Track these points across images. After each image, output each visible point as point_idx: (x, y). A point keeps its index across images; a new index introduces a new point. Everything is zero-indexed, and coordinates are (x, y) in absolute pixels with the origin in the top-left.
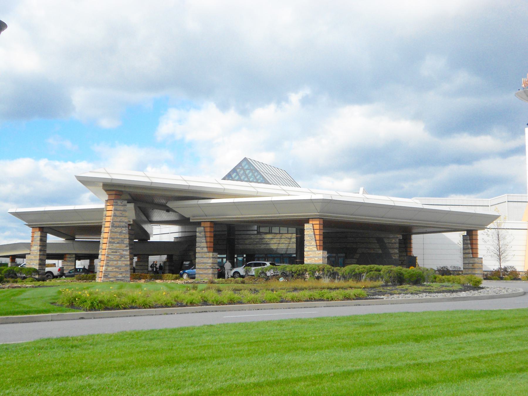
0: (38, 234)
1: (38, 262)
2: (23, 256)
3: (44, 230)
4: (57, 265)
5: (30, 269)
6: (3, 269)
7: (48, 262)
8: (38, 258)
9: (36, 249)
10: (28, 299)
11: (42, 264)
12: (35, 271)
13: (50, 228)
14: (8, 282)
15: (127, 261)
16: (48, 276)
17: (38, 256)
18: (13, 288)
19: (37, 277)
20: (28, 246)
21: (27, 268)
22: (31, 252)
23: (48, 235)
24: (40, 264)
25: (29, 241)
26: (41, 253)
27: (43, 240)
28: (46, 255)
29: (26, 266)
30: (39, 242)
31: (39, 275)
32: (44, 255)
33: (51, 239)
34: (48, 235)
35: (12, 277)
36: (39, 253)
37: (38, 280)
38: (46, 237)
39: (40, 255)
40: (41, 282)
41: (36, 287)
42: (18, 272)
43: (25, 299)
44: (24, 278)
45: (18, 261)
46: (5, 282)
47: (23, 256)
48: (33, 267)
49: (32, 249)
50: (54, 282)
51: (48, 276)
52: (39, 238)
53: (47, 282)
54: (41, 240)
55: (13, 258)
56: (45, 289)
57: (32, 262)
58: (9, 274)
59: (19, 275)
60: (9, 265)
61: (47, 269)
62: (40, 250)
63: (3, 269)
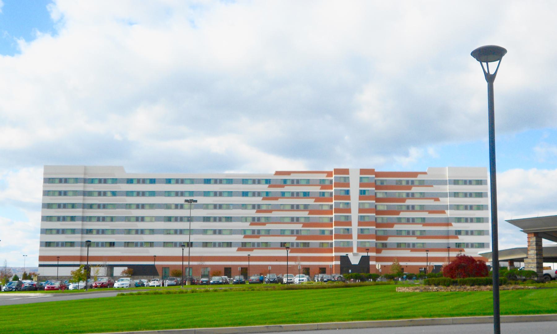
0: (534, 239)
1: (535, 265)
2: (521, 260)
3: (539, 236)
4: (552, 268)
5: (529, 271)
6: (504, 272)
7: (545, 265)
8: (535, 261)
9: (532, 253)
10: (536, 300)
11: (540, 267)
12: (533, 273)
13: (545, 233)
14: (511, 284)
15: (489, 314)
16: (545, 278)
17: (536, 260)
18: (517, 289)
19: (536, 279)
20: (525, 250)
21: (527, 271)
22: (529, 256)
23: (543, 239)
24: (537, 267)
25: (526, 246)
26: (538, 257)
27: (539, 244)
28: (543, 257)
29: (525, 269)
30: (535, 247)
31: (537, 277)
32: (540, 258)
33: (546, 243)
34: (543, 239)
35: (514, 280)
36: (536, 257)
37: (538, 282)
38: (541, 242)
39: (537, 258)
40: (541, 284)
41: (537, 288)
42: (518, 275)
43: (533, 300)
44: (525, 280)
45: (516, 264)
46: (508, 284)
47: (521, 260)
48: (532, 269)
49: (529, 253)
50: (552, 283)
51: (545, 278)
52: (534, 243)
53: (547, 284)
54: (537, 244)
55: (511, 262)
56: (547, 290)
57: (529, 265)
58: (510, 276)
59: (518, 277)
60: (509, 268)
61: (545, 272)
62: (537, 254)
63: (504, 272)
